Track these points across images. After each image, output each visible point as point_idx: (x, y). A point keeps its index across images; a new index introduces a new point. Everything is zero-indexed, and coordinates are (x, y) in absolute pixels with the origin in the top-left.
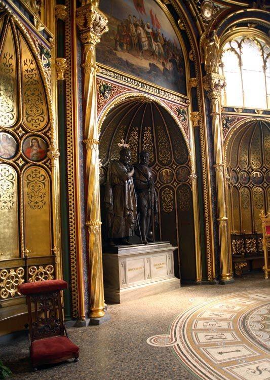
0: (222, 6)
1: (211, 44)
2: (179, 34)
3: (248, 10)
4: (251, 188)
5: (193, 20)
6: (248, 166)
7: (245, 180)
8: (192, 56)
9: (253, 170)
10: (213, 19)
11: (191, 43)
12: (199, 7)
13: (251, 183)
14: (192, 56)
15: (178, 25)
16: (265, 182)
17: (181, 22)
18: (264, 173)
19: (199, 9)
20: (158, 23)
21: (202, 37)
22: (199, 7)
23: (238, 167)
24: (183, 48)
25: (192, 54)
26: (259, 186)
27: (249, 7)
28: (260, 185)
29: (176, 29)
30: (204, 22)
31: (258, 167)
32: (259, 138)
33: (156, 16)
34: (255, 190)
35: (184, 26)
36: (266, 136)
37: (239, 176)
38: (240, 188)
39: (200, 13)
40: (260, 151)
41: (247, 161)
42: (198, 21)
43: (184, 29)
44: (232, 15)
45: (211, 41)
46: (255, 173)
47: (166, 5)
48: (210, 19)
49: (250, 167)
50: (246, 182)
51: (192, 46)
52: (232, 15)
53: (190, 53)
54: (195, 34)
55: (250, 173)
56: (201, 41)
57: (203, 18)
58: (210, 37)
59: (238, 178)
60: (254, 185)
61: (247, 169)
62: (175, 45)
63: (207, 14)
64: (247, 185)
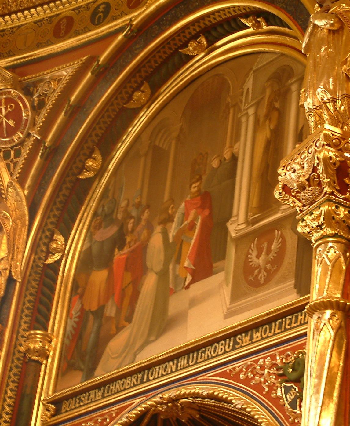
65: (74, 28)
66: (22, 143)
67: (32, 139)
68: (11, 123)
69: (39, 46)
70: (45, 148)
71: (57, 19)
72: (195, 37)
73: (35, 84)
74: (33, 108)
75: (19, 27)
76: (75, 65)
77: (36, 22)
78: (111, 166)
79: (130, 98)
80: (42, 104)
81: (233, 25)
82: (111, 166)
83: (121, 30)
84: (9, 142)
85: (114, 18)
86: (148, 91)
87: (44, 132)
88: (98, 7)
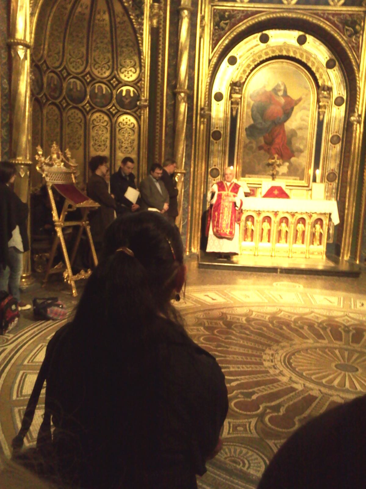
4: (64, 109)
6: (61, 64)
7: (54, 90)
9: (69, 74)
13: (64, 98)
16: (88, 102)
18: (88, 84)
23: (45, 62)
26: (77, 108)
28: (80, 106)
31: (79, 71)
32: (87, 12)
34: (70, 113)
36: (99, 13)
37: (45, 80)
38: (45, 104)
40: (85, 41)
41: (61, 54)
46: (72, 80)
49: (65, 68)
50: (56, 95)
55: (65, 79)
59: (43, 85)
60: (68, 104)
61: (60, 69)
64: (57, 101)
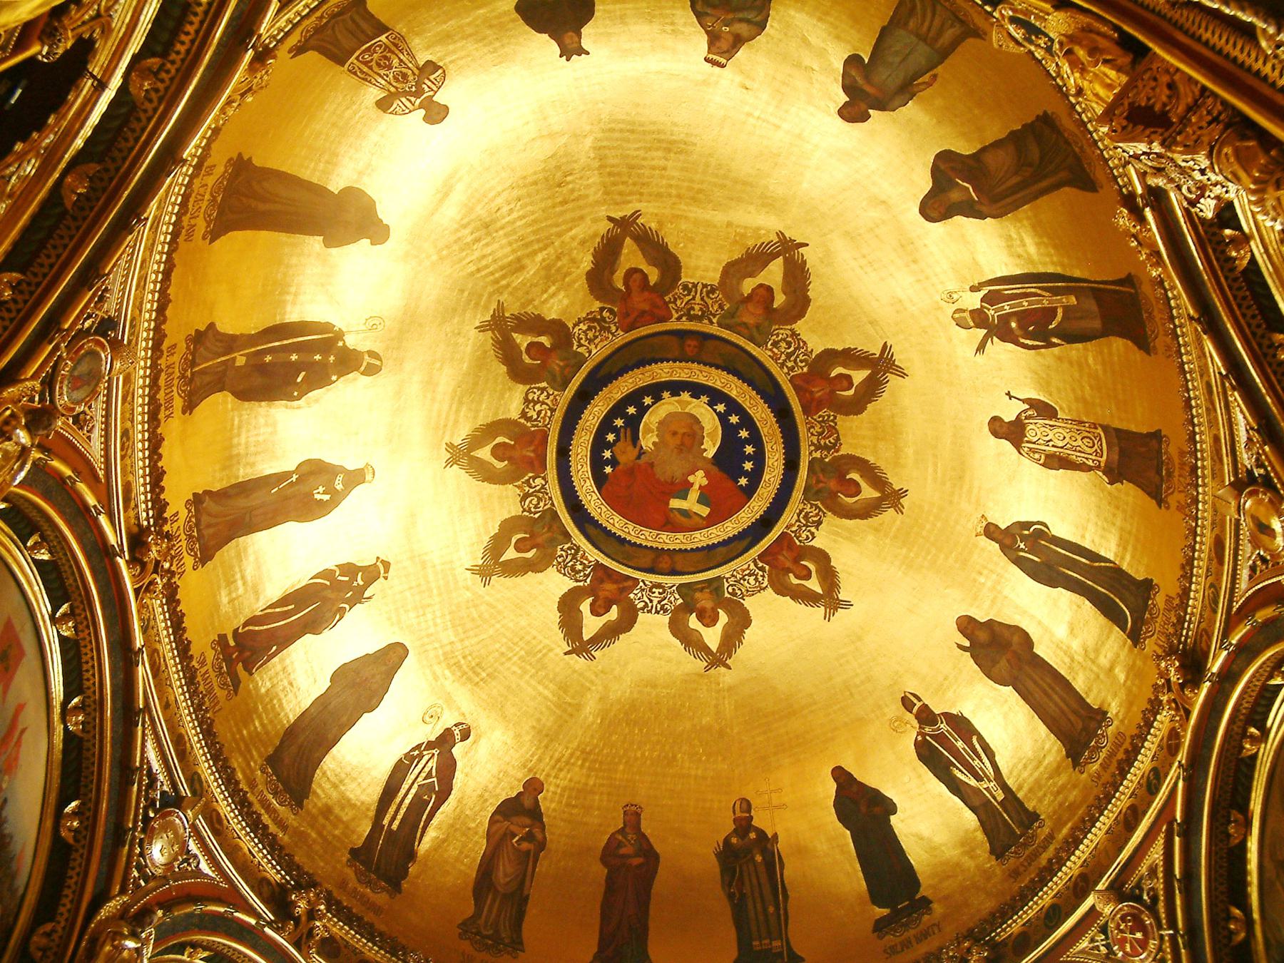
0: (204, 867)
1: (131, 944)
2: (46, 843)
3: (267, 930)
5: (118, 835)
8: (43, 941)
10: (164, 878)
11: (66, 901)
12: (152, 815)
14: (44, 941)
15: (59, 815)
17: (75, 814)
19: (146, 820)
20: (16, 759)
21: (111, 904)
22: (152, 815)
24: (31, 898)
25: (48, 935)
27: (270, 924)
29: (49, 823)
30: (140, 868)
33: (23, 731)
35: (76, 831)
39: (144, 830)
42: (127, 847)
43: (71, 841)
44: (222, 910)
45: (134, 935)
47: (66, 728)
48: (159, 872)
51: (62, 909)
52: (222, 910)
53: (41, 930)
54: (97, 879)
56: (104, 913)
57: (142, 854)
58: (137, 920)
62: (14, 866)
63: (158, 852)
65: (1140, 812)
66: (1160, 949)
67: (1167, 938)
68: (1139, 935)
69: (1121, 849)
70: (1182, 936)
71: (1122, 815)
72: (1244, 734)
73: (1138, 886)
74: (1148, 908)
75: (1096, 847)
76: (1160, 841)
77: (1107, 833)
78: (1256, 916)
79: (1228, 836)
80: (1155, 899)
81: (1268, 695)
82: (1256, 916)
83: (1178, 778)
84: (1149, 955)
85: (1166, 776)
86: (1240, 817)
87: (1172, 923)
88: (1148, 777)
